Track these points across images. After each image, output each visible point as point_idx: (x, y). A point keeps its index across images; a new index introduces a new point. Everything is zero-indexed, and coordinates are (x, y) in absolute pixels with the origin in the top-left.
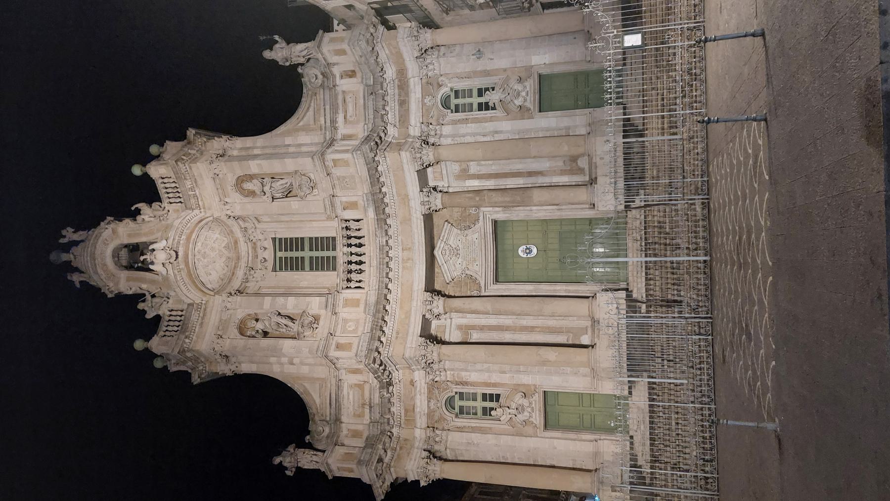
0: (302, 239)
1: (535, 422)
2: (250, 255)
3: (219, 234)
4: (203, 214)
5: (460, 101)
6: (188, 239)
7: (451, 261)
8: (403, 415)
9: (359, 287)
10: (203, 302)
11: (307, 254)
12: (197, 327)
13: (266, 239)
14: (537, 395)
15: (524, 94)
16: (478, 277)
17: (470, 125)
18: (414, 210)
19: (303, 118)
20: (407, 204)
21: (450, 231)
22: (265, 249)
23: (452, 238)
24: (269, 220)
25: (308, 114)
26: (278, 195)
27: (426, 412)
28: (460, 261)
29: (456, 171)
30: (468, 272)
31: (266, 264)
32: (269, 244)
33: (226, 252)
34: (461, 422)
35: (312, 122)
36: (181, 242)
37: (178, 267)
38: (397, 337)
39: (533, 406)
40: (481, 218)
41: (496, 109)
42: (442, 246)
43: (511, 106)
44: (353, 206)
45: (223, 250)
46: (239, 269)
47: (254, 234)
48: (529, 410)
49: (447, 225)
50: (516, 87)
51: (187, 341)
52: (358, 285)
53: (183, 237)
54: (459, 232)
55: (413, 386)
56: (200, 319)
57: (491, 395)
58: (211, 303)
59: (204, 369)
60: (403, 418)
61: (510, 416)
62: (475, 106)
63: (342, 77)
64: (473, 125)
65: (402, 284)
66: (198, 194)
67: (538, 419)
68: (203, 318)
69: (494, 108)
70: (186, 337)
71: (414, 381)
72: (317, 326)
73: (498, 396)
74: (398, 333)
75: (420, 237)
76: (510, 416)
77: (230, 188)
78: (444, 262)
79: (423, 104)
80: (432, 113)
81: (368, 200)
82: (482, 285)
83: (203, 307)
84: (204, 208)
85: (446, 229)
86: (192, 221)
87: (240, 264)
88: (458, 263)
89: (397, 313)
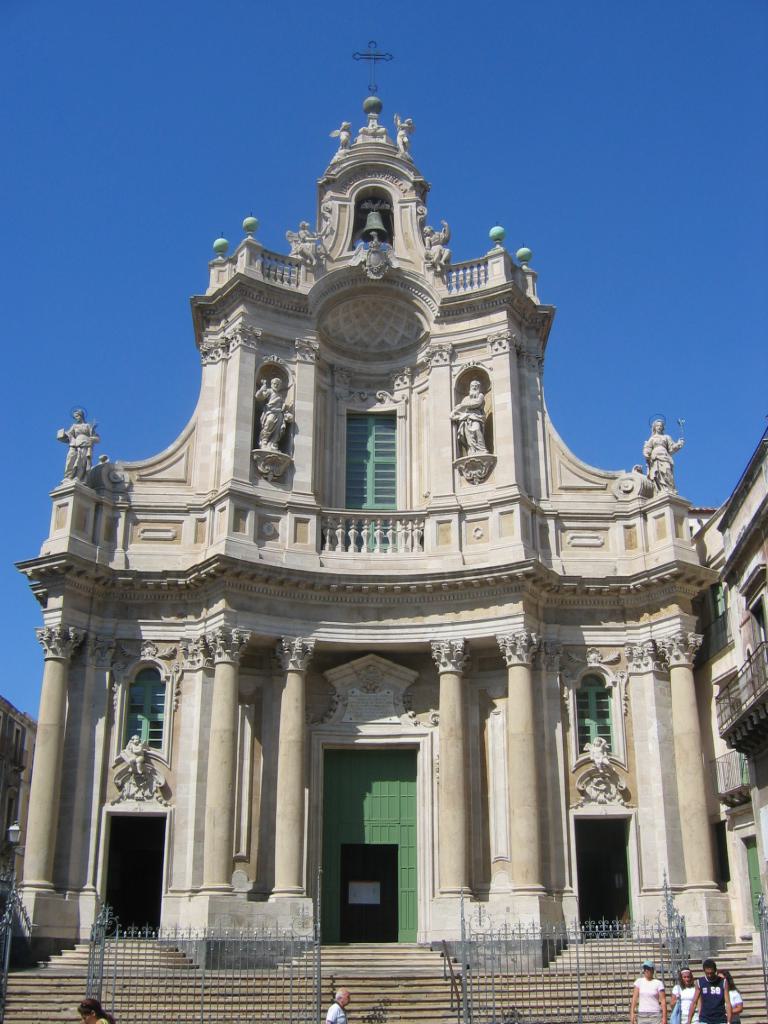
0: (393, 454)
3: (403, 337)
8: (134, 602)
24: (424, 409)
26: (461, 430)
28: (358, 692)
30: (340, 704)
31: (357, 399)
35: (564, 484)
36: (394, 287)
38: (251, 598)
44: (442, 537)
45: (379, 340)
47: (403, 386)
48: (139, 795)
51: (255, 294)
54: (401, 693)
57: (159, 735)
60: (130, 602)
63: (627, 527)
66: (464, 315)
67: (128, 807)
68: (286, 314)
69: (581, 751)
70: (260, 292)
73: (158, 745)
77: (471, 360)
81: (453, 561)
83: (301, 314)
88: (355, 690)
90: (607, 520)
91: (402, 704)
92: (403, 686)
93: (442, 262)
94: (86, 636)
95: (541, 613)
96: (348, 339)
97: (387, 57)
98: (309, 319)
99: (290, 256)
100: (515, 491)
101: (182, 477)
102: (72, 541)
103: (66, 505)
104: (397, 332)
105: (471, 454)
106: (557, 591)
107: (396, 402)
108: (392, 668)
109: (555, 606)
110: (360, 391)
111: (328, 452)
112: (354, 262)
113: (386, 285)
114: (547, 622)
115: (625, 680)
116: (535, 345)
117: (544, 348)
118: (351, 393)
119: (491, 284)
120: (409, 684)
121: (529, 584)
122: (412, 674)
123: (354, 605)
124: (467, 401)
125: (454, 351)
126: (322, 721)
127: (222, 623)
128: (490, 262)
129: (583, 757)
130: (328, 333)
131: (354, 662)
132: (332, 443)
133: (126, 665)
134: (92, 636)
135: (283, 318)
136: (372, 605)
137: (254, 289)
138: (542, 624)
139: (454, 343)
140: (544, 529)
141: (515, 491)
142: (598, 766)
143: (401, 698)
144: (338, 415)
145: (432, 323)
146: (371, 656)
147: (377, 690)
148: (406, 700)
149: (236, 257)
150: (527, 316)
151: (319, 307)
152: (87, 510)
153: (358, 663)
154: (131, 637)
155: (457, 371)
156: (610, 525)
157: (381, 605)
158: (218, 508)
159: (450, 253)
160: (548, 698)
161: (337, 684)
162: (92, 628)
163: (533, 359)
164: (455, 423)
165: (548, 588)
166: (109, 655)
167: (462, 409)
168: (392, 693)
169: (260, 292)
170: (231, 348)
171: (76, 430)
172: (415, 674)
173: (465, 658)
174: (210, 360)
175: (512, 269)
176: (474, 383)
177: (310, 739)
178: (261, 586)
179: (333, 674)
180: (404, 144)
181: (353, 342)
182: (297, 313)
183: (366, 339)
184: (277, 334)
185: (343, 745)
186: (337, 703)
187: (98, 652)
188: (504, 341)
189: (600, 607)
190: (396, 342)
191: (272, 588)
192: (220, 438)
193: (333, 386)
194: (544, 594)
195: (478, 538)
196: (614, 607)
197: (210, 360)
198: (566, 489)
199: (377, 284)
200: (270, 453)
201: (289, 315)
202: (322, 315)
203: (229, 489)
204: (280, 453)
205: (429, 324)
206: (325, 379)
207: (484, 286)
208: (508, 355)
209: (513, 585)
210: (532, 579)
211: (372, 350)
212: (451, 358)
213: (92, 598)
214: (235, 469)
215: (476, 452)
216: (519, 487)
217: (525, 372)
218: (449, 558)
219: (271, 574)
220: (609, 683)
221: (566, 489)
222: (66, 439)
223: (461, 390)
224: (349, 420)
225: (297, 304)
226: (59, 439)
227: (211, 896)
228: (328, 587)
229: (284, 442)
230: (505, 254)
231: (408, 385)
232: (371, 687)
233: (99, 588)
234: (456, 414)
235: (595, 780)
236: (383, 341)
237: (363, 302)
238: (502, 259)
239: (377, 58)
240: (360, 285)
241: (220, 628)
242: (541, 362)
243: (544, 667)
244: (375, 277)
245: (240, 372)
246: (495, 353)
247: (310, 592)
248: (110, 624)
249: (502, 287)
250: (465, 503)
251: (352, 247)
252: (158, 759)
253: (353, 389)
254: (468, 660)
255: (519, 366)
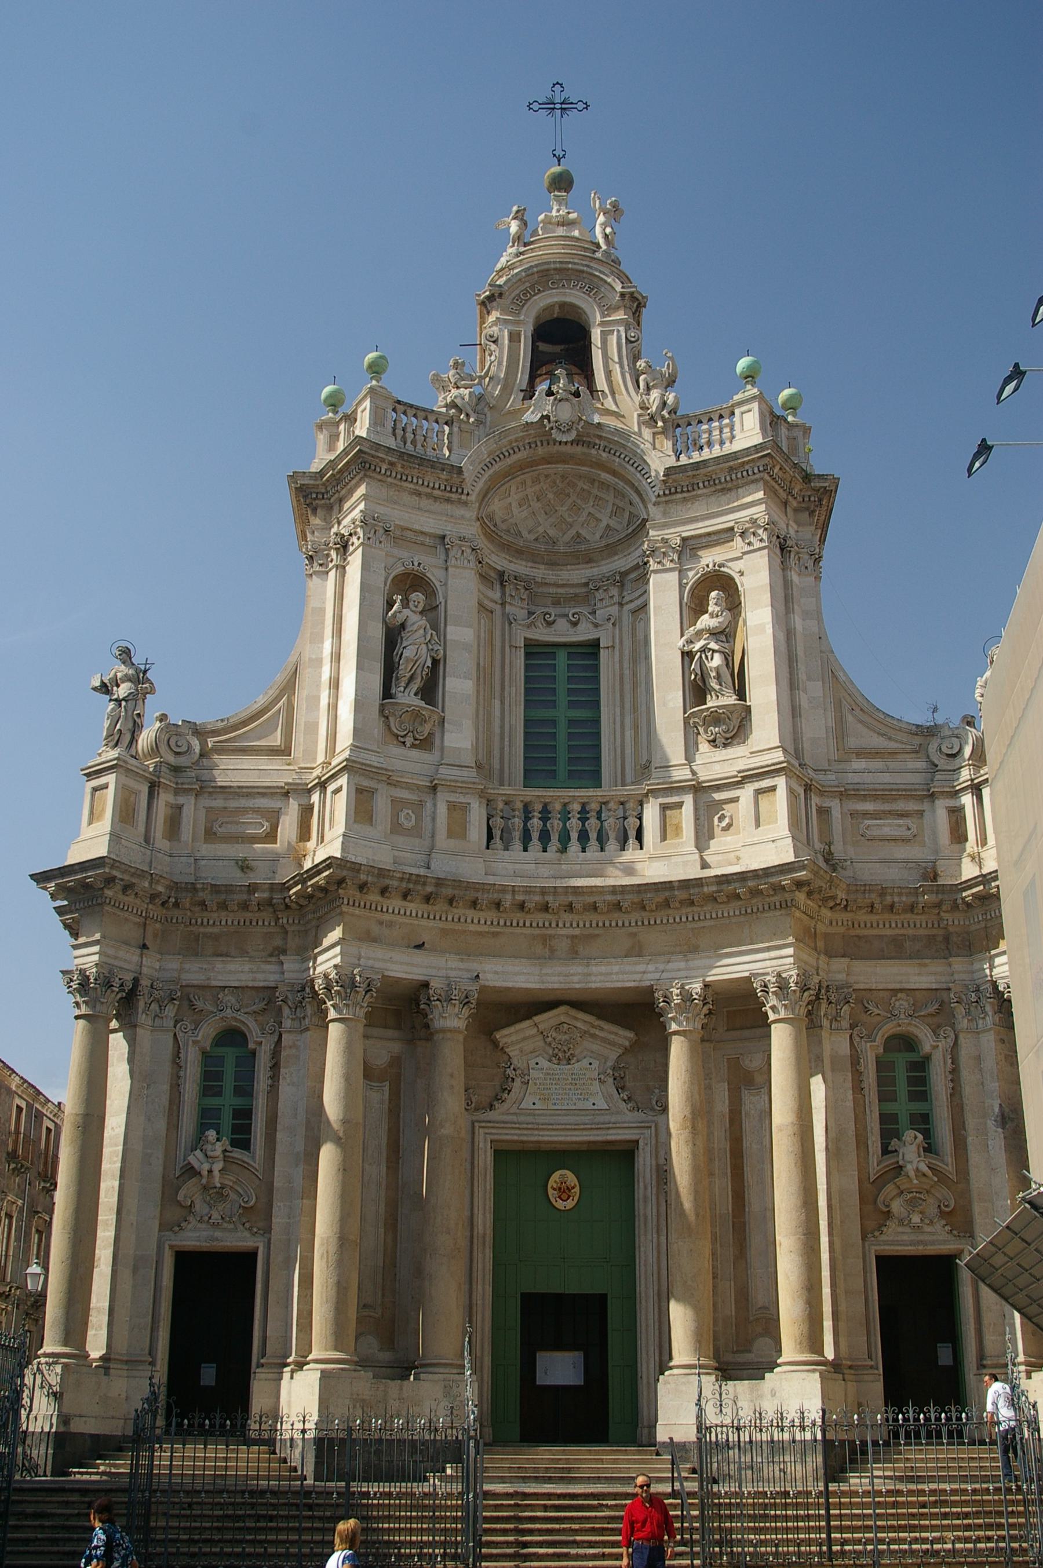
1: (190, 1226)
2: (561, 591)
4: (654, 499)
5: (901, 1075)
6: (601, 465)
7: (541, 1044)
8: (209, 930)
9: (490, 836)
10: (464, 497)
11: (562, 713)
12: (412, 486)
13: (596, 625)
14: (247, 1234)
15: (916, 1219)
16: (506, 1106)
17: (851, 1097)
18: (661, 967)
19: (861, 722)
20: (678, 949)
21: (613, 1044)
22: (575, 624)
23: (595, 1047)
25: (871, 733)
27: (214, 983)
28: (544, 1063)
29: (747, 1062)
30: (518, 1082)
32: (584, 633)
33: (567, 537)
34: (192, 1058)
35: (852, 742)
36: (593, 452)
37: (539, 444)
38: (381, 923)
39: (225, 1225)
40: (640, 1116)
41: (882, 1156)
42: (579, 1025)
43: (890, 1189)
45: (572, 532)
46: (530, 564)
49: (626, 1038)
50: (931, 1200)
51: (384, 467)
52: (497, 833)
53: (604, 455)
54: (610, 1064)
55: (271, 955)
56: (429, 490)
58: (460, 511)
59: (320, 496)
60: (202, 930)
61: (205, 1173)
62: (891, 1108)
64: (850, 1104)
65: (495, 934)
66: (700, 492)
68: (429, 496)
69: (885, 1151)
71: (282, 957)
72: (408, 745)
74: (390, 925)
75: (602, 978)
76: (205, 1173)
78: (541, 1027)
79: (895, 992)
80: (877, 1011)
81: (685, 863)
82: (491, 1115)
83: (453, 496)
84: (666, 502)
85: (616, 1034)
86: (638, 475)
87: (543, 567)
88: (540, 1060)
89: (431, 923)
90: (921, 799)
91: (611, 1080)
92: (613, 1055)
93: (665, 413)
94: (136, 981)
95: (820, 944)
96: (525, 534)
97: (581, 106)
98: (465, 503)
99: (435, 409)
100: (779, 756)
101: (276, 739)
102: (115, 837)
103: (105, 786)
104: (599, 520)
105: (711, 702)
106: (846, 906)
107: (596, 625)
108: (593, 1026)
109: (842, 930)
110: (546, 610)
111: (497, 703)
112: (531, 416)
113: (579, 449)
114: (830, 954)
115: (950, 1042)
116: (809, 536)
117: (822, 540)
118: (531, 613)
119: (738, 445)
120: (621, 1051)
121: (801, 897)
122: (624, 1036)
123: (537, 931)
124: (705, 621)
125: (690, 547)
126: (491, 1107)
127: (338, 960)
128: (737, 411)
129: (890, 1160)
130: (495, 525)
131: (537, 1019)
132: (503, 688)
133: (197, 1025)
134: (145, 982)
135: (425, 503)
136: (564, 932)
137: (383, 460)
138: (822, 957)
139: (684, 535)
140: (824, 812)
141: (779, 756)
142: (912, 1174)
143: (610, 1071)
144: (510, 646)
145: (650, 506)
146: (563, 1009)
147: (572, 1062)
148: (616, 1074)
149: (355, 411)
150: (795, 492)
151: (480, 484)
152: (136, 793)
153: (546, 1020)
154: (206, 983)
155: (692, 577)
156: (926, 806)
157: (577, 932)
158: (331, 788)
159: (676, 397)
160: (833, 1070)
161: (513, 1052)
162: (145, 970)
163: (807, 557)
164: (687, 656)
165: (832, 904)
166: (170, 1011)
167: (699, 634)
168: (596, 1064)
169: (391, 464)
170: (351, 549)
171: (119, 675)
172: (631, 1035)
173: (705, 1010)
174: (318, 568)
175: (772, 420)
176: (713, 594)
177: (473, 1133)
178: (395, 903)
179: (506, 1036)
180: (606, 236)
181: (532, 537)
182: (448, 495)
183: (552, 532)
184: (416, 527)
185: (522, 1142)
186: (513, 1079)
187: (154, 1006)
188: (760, 531)
189: (911, 932)
190: (598, 536)
191: (412, 907)
192: (335, 684)
193: (503, 604)
194: (826, 913)
195: (725, 829)
196: (935, 932)
197: (318, 568)
198: (861, 753)
199: (568, 449)
200: (410, 706)
201: (436, 499)
202: (485, 495)
203: (346, 760)
204: (423, 704)
205: (646, 507)
206: (490, 593)
207: (730, 448)
208: (766, 551)
209: (776, 899)
210: (806, 889)
211: (562, 549)
212: (679, 559)
213: (145, 924)
214: (355, 729)
215: (722, 700)
216: (785, 750)
217: (795, 578)
218: (680, 859)
219: (411, 886)
220: (927, 1048)
221: (861, 753)
222: (104, 688)
223: (695, 606)
224: (528, 655)
225: (447, 480)
226: (95, 689)
227: (323, 1371)
228: (498, 905)
229: (430, 691)
230: (760, 398)
231: (616, 599)
232: (564, 1056)
233: (156, 911)
234: (690, 642)
235: (909, 1196)
236: (578, 535)
237: (547, 476)
238: (755, 406)
239: (566, 106)
240: (541, 451)
241: (335, 966)
242: (817, 560)
243: (826, 1023)
244: (564, 438)
245: (362, 583)
246: (746, 548)
247: (470, 913)
248: (173, 964)
249: (757, 448)
250: (705, 775)
251: (529, 393)
252: (244, 1166)
253: (533, 608)
254: (710, 1012)
255: (784, 566)
